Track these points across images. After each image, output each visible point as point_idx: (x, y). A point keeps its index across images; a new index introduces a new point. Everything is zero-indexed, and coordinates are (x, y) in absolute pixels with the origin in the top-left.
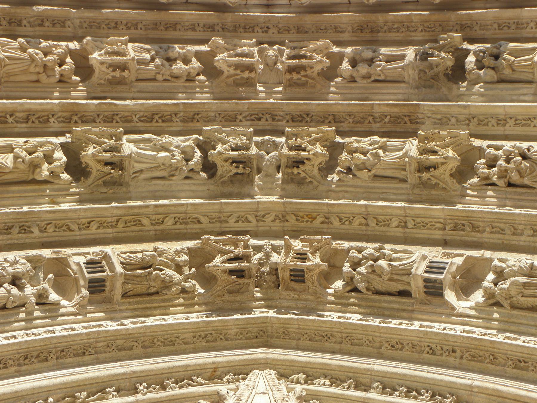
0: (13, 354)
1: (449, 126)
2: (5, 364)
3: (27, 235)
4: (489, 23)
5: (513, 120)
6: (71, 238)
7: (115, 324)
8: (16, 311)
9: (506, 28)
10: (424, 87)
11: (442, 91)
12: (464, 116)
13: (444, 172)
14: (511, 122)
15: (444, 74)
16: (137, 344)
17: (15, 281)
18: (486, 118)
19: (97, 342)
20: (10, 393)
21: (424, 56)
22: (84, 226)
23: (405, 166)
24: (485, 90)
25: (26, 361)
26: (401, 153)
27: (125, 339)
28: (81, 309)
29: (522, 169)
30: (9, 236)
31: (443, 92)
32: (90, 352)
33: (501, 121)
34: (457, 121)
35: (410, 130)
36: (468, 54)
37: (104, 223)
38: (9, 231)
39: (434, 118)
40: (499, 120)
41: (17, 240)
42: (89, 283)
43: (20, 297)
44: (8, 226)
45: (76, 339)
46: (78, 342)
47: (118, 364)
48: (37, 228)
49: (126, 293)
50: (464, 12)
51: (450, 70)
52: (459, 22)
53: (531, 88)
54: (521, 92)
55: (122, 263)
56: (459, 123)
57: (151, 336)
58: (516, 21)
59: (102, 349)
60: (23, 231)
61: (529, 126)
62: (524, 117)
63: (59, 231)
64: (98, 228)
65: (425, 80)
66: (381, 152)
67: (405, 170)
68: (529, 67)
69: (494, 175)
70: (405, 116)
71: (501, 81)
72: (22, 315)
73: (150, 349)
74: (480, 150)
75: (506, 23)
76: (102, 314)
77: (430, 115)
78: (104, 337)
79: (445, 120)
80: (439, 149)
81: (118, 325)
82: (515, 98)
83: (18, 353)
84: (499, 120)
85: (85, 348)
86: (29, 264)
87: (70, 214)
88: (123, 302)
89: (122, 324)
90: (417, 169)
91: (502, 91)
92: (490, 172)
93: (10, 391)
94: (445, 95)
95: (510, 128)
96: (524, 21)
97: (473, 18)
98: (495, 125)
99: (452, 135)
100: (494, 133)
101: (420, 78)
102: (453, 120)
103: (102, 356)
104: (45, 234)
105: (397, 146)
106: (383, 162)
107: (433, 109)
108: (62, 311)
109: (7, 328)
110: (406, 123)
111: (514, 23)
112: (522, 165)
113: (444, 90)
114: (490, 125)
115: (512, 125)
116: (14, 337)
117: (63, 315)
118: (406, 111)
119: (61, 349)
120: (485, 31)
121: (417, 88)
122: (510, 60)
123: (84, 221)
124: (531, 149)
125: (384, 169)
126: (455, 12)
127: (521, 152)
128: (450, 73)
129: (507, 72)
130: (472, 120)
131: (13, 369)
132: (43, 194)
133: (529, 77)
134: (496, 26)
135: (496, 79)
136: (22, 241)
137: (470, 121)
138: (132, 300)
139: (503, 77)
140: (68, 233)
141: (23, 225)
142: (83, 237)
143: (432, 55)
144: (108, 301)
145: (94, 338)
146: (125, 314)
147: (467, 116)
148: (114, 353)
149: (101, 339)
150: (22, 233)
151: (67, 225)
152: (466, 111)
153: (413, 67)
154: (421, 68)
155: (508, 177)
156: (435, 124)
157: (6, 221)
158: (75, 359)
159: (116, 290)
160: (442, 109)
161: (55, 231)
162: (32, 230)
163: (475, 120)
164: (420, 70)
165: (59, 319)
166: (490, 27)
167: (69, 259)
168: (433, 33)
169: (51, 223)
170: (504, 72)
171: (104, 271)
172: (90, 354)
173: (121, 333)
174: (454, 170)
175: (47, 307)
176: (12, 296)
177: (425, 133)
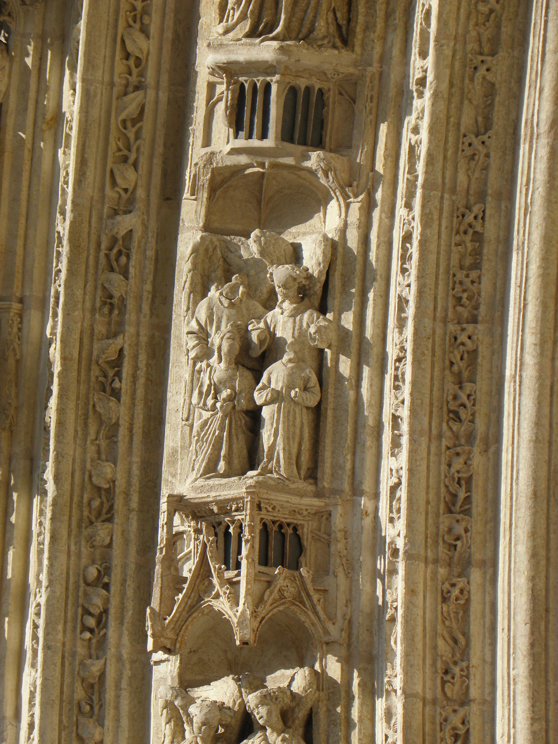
0: (439, 455)
2: (459, 483)
3: (134, 251)
6: (161, 119)
7: (417, 103)
8: (331, 380)
16: (482, 71)
17: (253, 358)
19: (453, 191)
20: (535, 514)
22: (135, 71)
25: (463, 416)
27: (462, 102)
28: (359, 183)
30: (131, 304)
32: (476, 218)
37: (134, 9)
38: (115, 301)
41: (143, 281)
42: (291, 140)
43: (298, 361)
44: (105, 303)
45: (433, 257)
46: (443, 248)
47: (523, 148)
48: (119, 218)
49: (339, 27)
55: (253, 33)
57: (468, 18)
59: (477, 175)
60: (123, 259)
63: (138, 150)
64: (145, 31)
72: (345, 366)
73: (503, 29)
76: (383, 128)
78: (444, 167)
81: (421, 95)
83: (440, 436)
85: (462, 228)
86: (213, 293)
87: (95, 113)
88: (363, 46)
89: (422, 82)
93: (528, 513)
103: (494, 181)
104: (141, 193)
108: (353, 240)
109: (371, 422)
116: (395, 419)
117: (365, 241)
119: (451, 302)
123: (120, 66)
131: (478, 461)
132: (29, 145)
136: (150, 267)
138: (361, 19)
140: (147, 124)
141: (107, 256)
142: (165, 79)
144: (350, 89)
145: (442, 197)
146: (396, 52)
148: (492, 143)
149: (448, 174)
150: (127, 266)
151: (124, 122)
157: (88, 305)
158: (486, 266)
159: (326, 67)
161: (135, 165)
162: (122, 233)
165: (373, 256)
167: (219, 162)
169: (112, 172)
171: (268, 87)
172: (483, 218)
173: (443, 116)
175: (336, 281)
176: (290, 387)
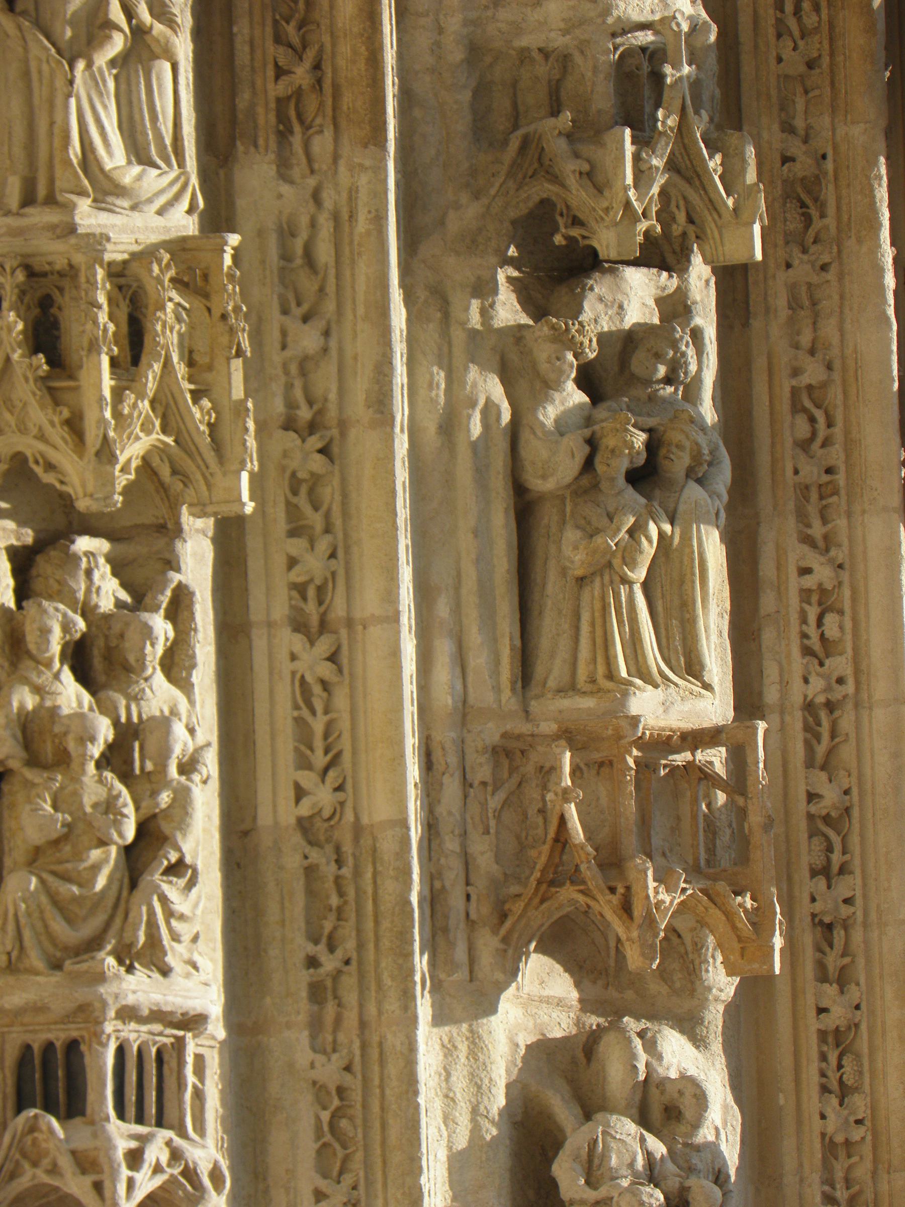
1: (275, 318)
4: (829, 329)
5: (326, 670)
9: (803, 428)
10: (481, 91)
11: (464, 198)
12: (333, 396)
13: (31, 427)
14: (312, 661)
15: (546, 204)
18: (327, 516)
21: (638, 83)
23: (51, 200)
24: (474, 445)
26: (114, 157)
29: (79, 855)
31: (457, 206)
33: (319, 616)
34: (305, 365)
35: (243, 99)
36: (664, 266)
39: (313, 224)
40: (321, 590)
50: (882, 194)
51: (571, 240)
52: (829, 165)
53: (497, 689)
54: (475, 637)
56: (294, 369)
58: (841, 478)
61: (304, 764)
62: (345, 724)
65: (515, 84)
66: (117, 44)
67: (28, 200)
68: (601, 670)
69: (38, 690)
70: (317, 66)
71: (525, 508)
74: (161, 528)
75: (830, 425)
77: (328, 204)
79: (308, 285)
80: (151, 386)
82: (443, 609)
84: (321, 590)
90: (39, 264)
91: (476, 533)
92: (49, 664)
94: (442, 223)
95: (283, 655)
96: (841, 523)
97: (850, 244)
98: (298, 576)
99: (225, 432)
100: (255, 565)
101: (524, 55)
102: (308, 340)
105: (154, 118)
106: (60, 83)
107: (362, 224)
110: (280, 72)
111: (829, 471)
112: (95, 854)
113: (467, 214)
114: (296, 546)
115: (300, 666)
118: (341, 62)
120: (784, 313)
121: (475, 51)
122: (633, 564)
124: (182, 882)
125: (26, 74)
126: (881, 145)
127: (166, 827)
128: (558, 239)
129: (568, 550)
130: (315, 442)
133: (552, 667)
134: (813, 373)
135: (538, 484)
137: (313, 427)
139: (548, 516)
143: (645, 140)
147: (332, 412)
152: (358, 407)
153: (582, 22)
154: (578, 59)
155: (30, 774)
156: (287, 232)
160: (363, 270)
163: (318, 463)
164: (565, 60)
166: (806, 339)
168: (771, 32)
170: (571, 535)
174: (48, 478)
177: (231, 277)
